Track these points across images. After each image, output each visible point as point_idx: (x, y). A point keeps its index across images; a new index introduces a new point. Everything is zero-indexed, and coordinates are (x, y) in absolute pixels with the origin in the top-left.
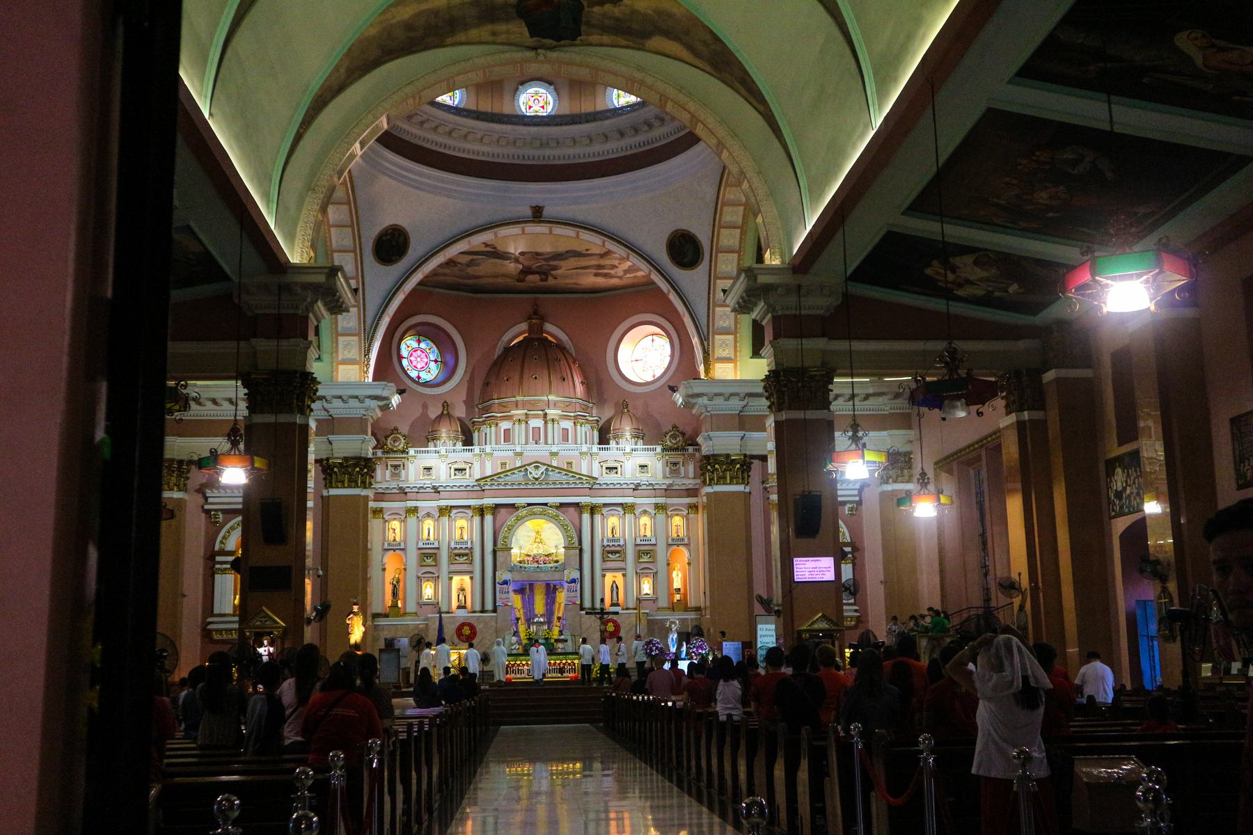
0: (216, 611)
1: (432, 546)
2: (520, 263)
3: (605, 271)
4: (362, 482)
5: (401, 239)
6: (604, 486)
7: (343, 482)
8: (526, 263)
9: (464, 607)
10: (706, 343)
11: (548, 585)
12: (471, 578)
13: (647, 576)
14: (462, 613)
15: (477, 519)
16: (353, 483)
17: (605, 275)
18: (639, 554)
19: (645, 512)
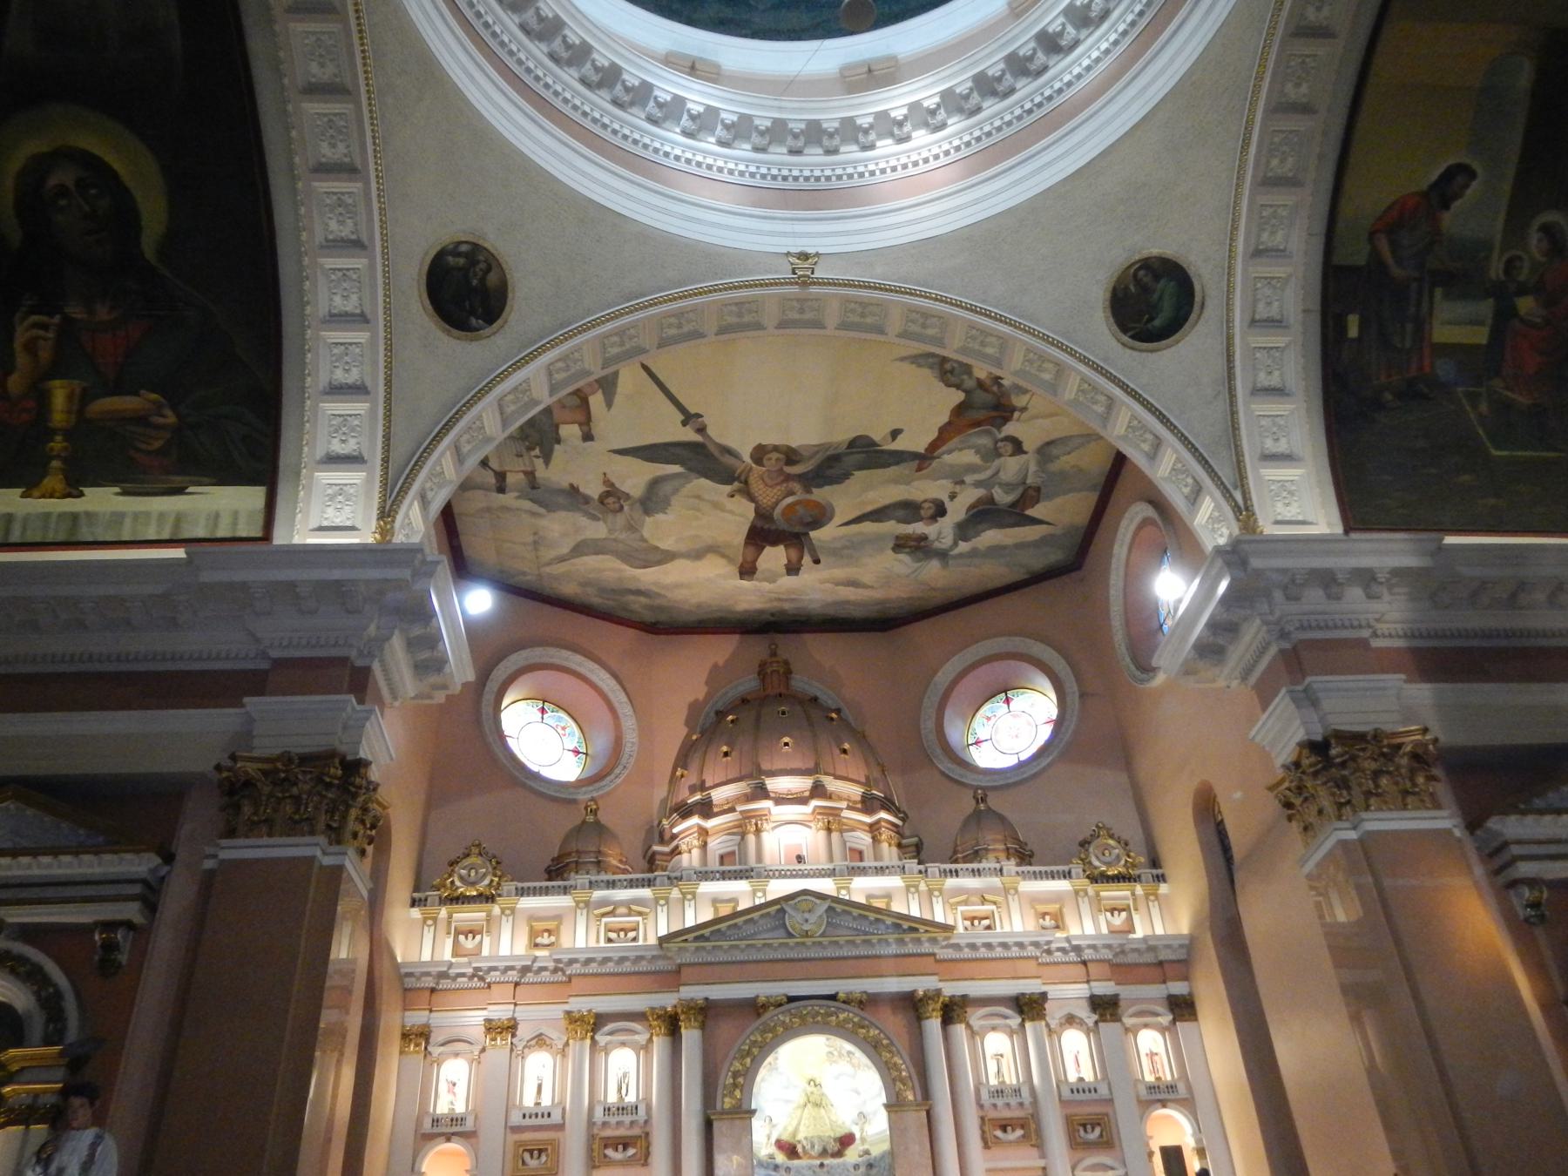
1: (546, 1121)
2: (752, 498)
3: (918, 528)
4: (329, 827)
5: (492, 278)
6: (967, 953)
8: (766, 495)
10: (1238, 496)
15: (660, 1044)
16: (297, 826)
17: (917, 547)
19: (1071, 1020)
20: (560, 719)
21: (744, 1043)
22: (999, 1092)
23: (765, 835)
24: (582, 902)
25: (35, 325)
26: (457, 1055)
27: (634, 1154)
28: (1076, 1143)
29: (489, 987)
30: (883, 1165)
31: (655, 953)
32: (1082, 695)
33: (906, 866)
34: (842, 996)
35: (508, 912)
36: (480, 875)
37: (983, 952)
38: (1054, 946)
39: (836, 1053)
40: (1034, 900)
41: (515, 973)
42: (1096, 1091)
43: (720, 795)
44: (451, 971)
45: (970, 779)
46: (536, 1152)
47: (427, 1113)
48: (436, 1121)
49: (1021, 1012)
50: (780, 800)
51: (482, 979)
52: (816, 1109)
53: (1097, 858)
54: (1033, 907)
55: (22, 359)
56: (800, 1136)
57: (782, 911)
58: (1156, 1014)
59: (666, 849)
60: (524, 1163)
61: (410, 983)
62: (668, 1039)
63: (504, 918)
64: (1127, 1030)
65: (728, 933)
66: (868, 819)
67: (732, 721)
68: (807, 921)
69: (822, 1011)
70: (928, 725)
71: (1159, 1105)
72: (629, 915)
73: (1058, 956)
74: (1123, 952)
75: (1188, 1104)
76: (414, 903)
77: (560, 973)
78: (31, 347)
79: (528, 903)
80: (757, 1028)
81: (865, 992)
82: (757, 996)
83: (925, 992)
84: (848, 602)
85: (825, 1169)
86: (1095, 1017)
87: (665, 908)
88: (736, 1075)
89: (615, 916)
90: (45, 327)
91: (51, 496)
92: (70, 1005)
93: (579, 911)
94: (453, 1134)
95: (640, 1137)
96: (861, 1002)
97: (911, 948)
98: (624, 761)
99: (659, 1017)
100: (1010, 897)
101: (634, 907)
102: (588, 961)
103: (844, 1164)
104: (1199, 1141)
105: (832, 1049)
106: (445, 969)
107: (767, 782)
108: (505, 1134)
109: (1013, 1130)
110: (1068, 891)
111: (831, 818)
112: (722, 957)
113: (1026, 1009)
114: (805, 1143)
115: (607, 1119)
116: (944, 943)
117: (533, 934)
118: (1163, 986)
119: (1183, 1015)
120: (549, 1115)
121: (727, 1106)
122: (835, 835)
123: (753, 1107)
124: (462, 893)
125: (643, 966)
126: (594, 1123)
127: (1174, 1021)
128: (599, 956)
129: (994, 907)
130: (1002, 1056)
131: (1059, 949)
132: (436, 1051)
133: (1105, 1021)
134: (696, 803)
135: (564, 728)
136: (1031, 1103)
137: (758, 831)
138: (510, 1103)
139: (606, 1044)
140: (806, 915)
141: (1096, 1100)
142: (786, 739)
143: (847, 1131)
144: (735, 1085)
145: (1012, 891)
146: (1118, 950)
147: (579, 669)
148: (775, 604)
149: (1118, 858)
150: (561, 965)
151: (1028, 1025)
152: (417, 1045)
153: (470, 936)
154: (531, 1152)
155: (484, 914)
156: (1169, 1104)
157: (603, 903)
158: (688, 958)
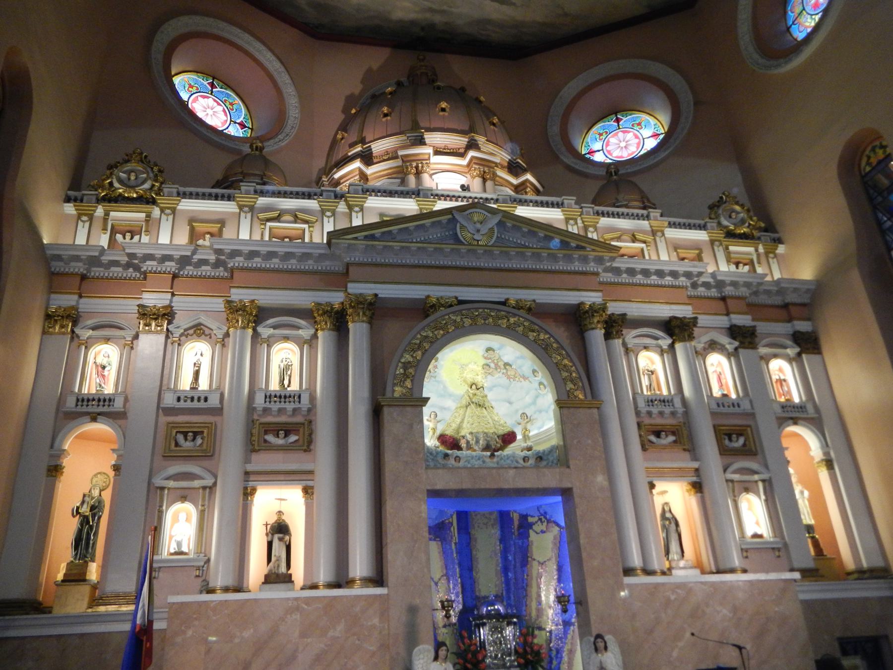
1: (202, 405)
9: (287, 579)
11: (504, 518)
12: (307, 491)
13: (747, 490)
14: (278, 593)
15: (325, 340)
18: (724, 434)
19: (713, 346)
20: (228, 96)
21: (414, 337)
22: (650, 401)
23: (425, 177)
24: (246, 206)
26: (107, 340)
27: (296, 441)
28: (724, 451)
29: (145, 279)
30: (551, 459)
31: (322, 251)
32: (696, 103)
33: (565, 201)
34: (513, 302)
35: (168, 211)
36: (140, 181)
37: (639, 278)
38: (702, 279)
39: (492, 365)
40: (676, 247)
41: (173, 264)
42: (739, 406)
43: (379, 147)
44: (103, 258)
45: (591, 170)
46: (190, 434)
47: (72, 392)
48: (83, 400)
49: (671, 334)
50: (437, 152)
51: (137, 268)
52: (479, 409)
53: (725, 218)
54: (676, 251)
56: (462, 433)
57: (453, 221)
58: (785, 347)
60: (177, 445)
61: (57, 266)
62: (334, 334)
63: (164, 217)
64: (762, 358)
65: (399, 238)
66: (515, 181)
67: (391, 93)
68: (478, 231)
69: (492, 314)
70: (554, 130)
71: (791, 422)
72: (295, 222)
73: (701, 291)
74: (756, 293)
75: (816, 423)
76: (68, 200)
77: (221, 269)
79: (187, 205)
80: (428, 325)
81: (534, 301)
82: (428, 297)
83: (590, 306)
84: (489, 21)
85: (495, 460)
86: (737, 344)
88: (406, 366)
89: (279, 222)
93: (243, 214)
94: (99, 414)
95: (303, 424)
96: (529, 310)
97: (577, 266)
98: (287, 130)
99: (325, 312)
100: (658, 239)
101: (300, 215)
102: (252, 254)
103: (513, 457)
104: (826, 454)
105: (488, 361)
106: (97, 254)
107: (425, 136)
108: (157, 416)
109: (667, 436)
110: (705, 241)
111: (486, 169)
112: (392, 259)
113: (677, 331)
114: (469, 437)
115: (268, 405)
116: (608, 264)
117: (194, 235)
118: (789, 325)
119: (808, 349)
120: (206, 399)
121: (396, 395)
122: (489, 184)
123: (425, 395)
124: (120, 195)
125: (310, 265)
126: (255, 408)
127: (799, 354)
128: (264, 250)
129: (643, 245)
130: (652, 372)
131: (706, 285)
132: (84, 334)
133: (745, 348)
135: (231, 104)
136: (684, 411)
137: (418, 174)
138: (164, 388)
139: (269, 337)
140: (478, 226)
141: (739, 414)
142: (444, 105)
143: (509, 429)
144: (406, 376)
145: (659, 234)
146: (755, 289)
147: (246, 47)
148: (428, 15)
149: (743, 222)
150: (223, 257)
151: (678, 346)
152: (62, 327)
153: (128, 235)
154: (185, 434)
155: (142, 216)
156: (800, 422)
157: (267, 209)
158: (357, 257)
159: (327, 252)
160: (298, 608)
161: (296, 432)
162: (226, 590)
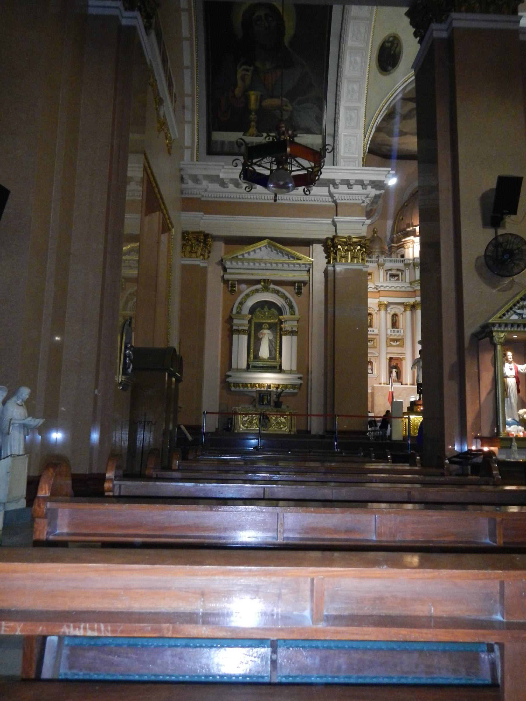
0: (234, 366)
1: (373, 333)
5: (397, 50)
7: (347, 258)
25: (244, 70)
55: (240, 83)
59: (396, 245)
78: (243, 78)
87: (408, 270)
90: (247, 70)
91: (253, 136)
92: (295, 304)
115: (391, 333)
125: (403, 289)
134: (410, 231)
159: (410, 286)
160: (405, 390)
161: (399, 341)
162: (384, 384)
